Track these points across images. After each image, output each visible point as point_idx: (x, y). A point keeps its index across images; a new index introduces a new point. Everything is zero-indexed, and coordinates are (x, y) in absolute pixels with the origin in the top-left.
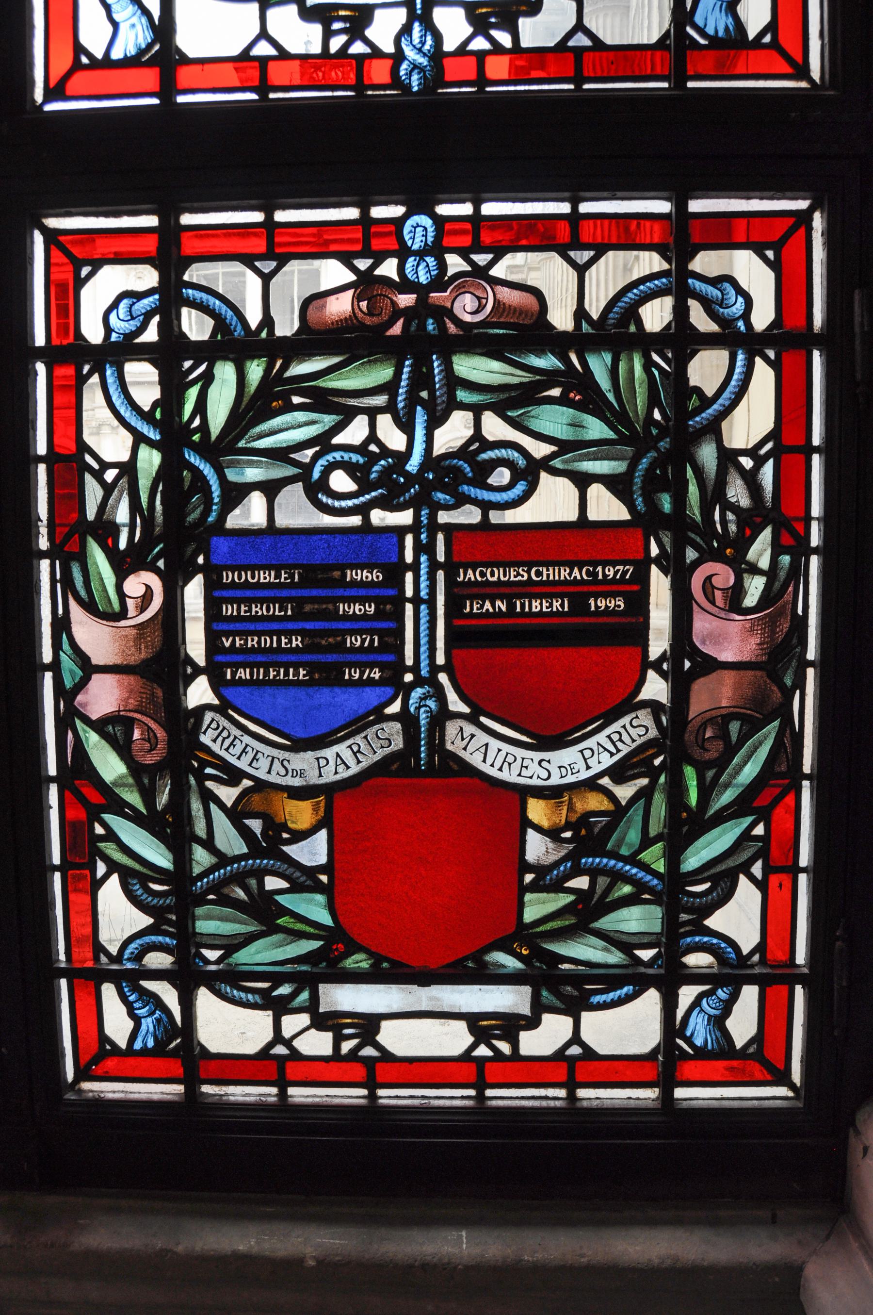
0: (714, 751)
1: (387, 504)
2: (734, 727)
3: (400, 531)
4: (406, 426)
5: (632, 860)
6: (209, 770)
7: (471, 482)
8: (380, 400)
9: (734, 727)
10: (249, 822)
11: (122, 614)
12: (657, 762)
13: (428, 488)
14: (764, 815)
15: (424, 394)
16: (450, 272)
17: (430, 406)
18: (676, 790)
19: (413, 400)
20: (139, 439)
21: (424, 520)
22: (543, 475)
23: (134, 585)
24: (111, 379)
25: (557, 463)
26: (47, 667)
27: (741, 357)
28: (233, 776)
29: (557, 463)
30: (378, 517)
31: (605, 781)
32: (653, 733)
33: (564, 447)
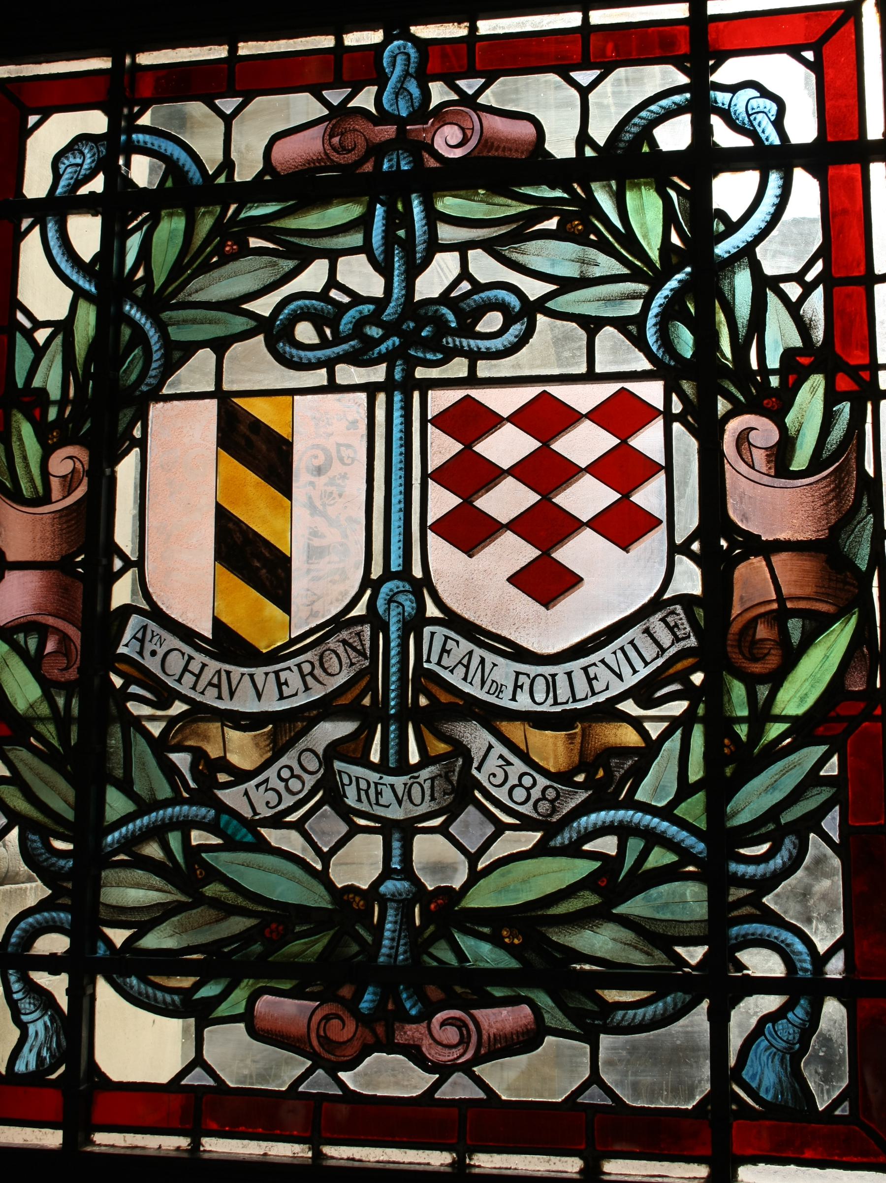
0: (773, 661)
1: (356, 359)
3: (371, 389)
5: (666, 813)
6: (134, 689)
7: (454, 333)
10: (175, 757)
11: (45, 499)
15: (401, 233)
16: (435, 102)
19: (389, 238)
21: (398, 375)
22: (541, 320)
24: (52, 234)
25: (558, 304)
29: (558, 304)
31: (629, 707)
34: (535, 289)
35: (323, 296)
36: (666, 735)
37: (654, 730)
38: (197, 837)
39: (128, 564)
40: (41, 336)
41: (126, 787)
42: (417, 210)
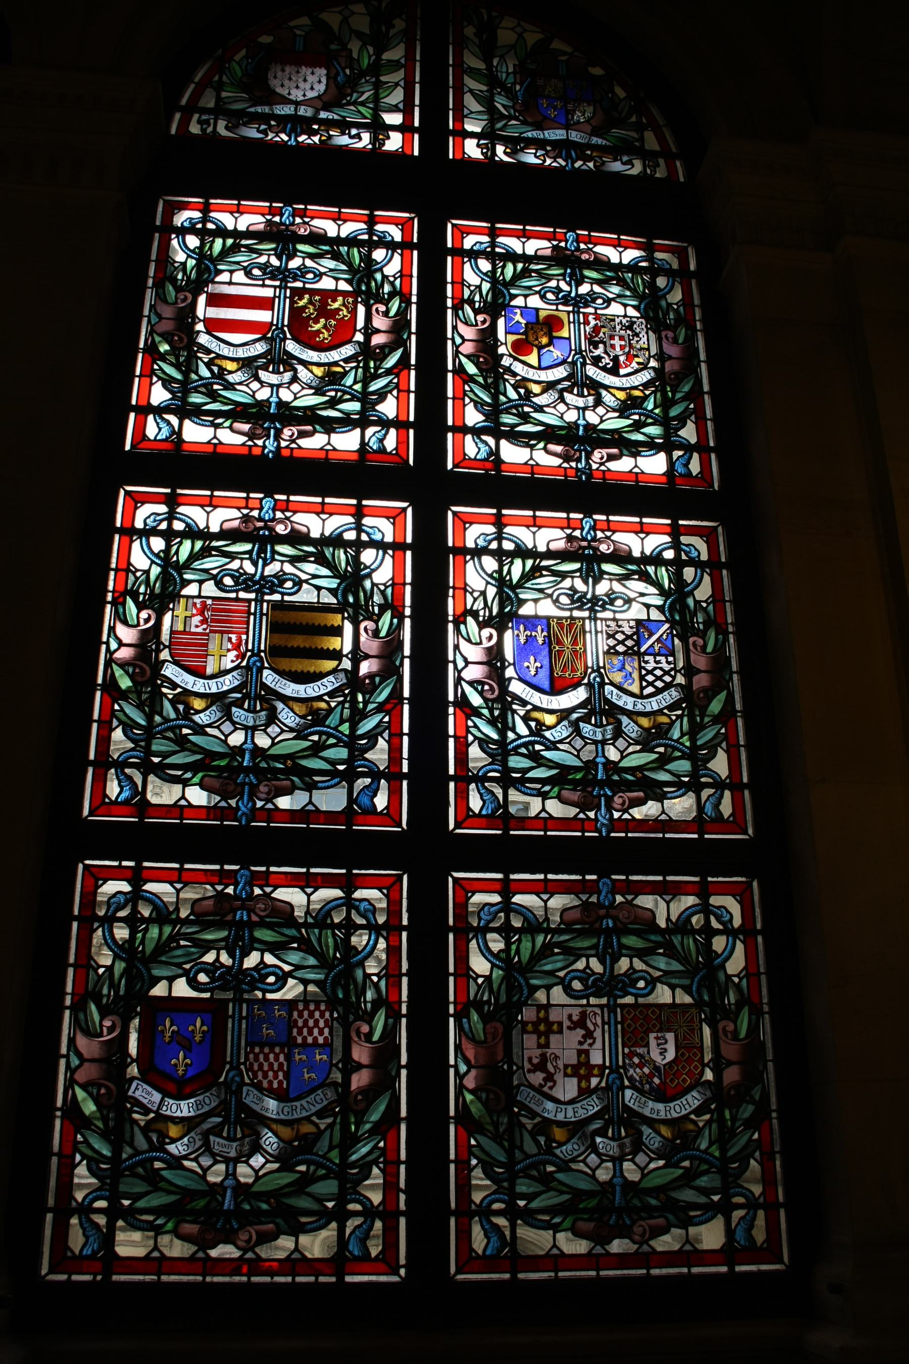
2: (377, 679)
4: (255, 564)
7: (278, 586)
8: (247, 556)
9: (377, 679)
11: (138, 625)
12: (347, 692)
13: (263, 587)
14: (388, 713)
17: (265, 560)
18: (354, 701)
20: (153, 562)
23: (144, 615)
26: (104, 643)
27: (381, 552)
28: (174, 686)
29: (311, 581)
30: (242, 595)
31: (326, 698)
32: (345, 681)
33: (315, 577)
34: (304, 577)
35: (237, 571)
36: (336, 707)
37: (333, 704)
38: (185, 731)
39: (165, 647)
40: (138, 574)
41: (161, 715)
42: (269, 548)
